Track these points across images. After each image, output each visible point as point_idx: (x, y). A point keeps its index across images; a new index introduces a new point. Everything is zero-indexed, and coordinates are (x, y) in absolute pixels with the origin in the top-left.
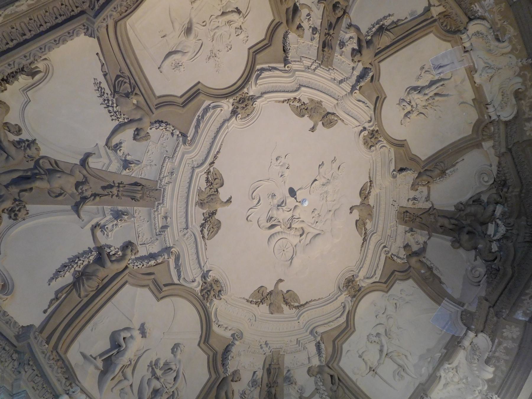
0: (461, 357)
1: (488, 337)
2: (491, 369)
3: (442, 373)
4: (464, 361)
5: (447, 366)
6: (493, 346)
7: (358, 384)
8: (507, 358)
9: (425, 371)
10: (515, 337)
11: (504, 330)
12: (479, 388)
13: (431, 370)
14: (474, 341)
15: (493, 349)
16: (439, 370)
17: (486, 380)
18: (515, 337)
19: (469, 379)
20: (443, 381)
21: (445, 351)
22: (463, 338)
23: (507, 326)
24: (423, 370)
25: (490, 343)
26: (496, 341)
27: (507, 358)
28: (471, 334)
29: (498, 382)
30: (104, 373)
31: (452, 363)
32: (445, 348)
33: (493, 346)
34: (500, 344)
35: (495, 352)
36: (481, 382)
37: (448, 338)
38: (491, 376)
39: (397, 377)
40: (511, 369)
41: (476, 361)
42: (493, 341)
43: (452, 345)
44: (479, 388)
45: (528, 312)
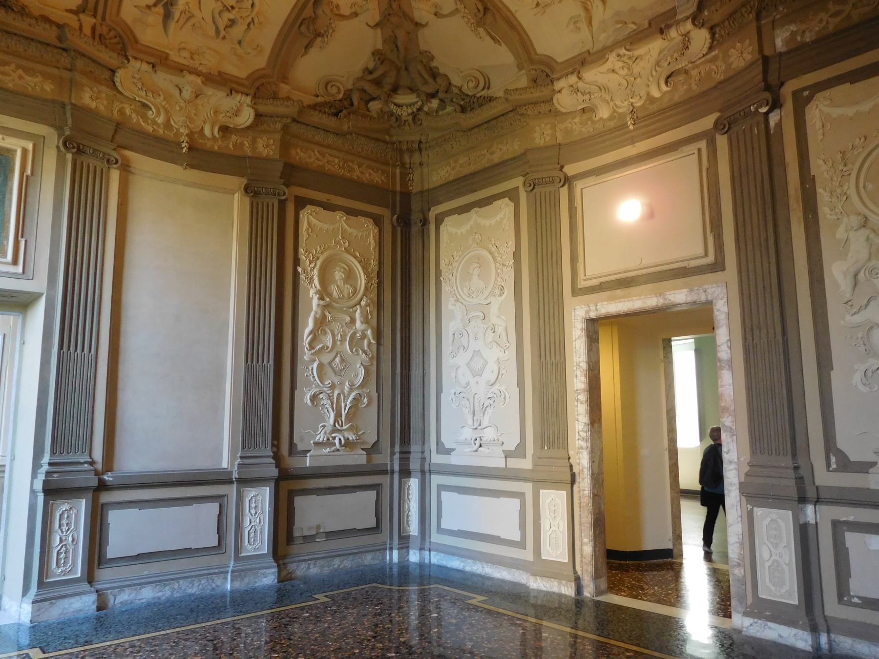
0: (654, 47)
1: (558, 107)
2: (664, 88)
3: (612, 57)
4: (655, 53)
5: (623, 51)
6: (704, 56)
7: (517, 15)
8: (694, 87)
9: (603, 39)
10: (734, 66)
11: (738, 45)
12: (631, 100)
13: (609, 42)
14: (692, 34)
15: (698, 63)
16: (611, 51)
17: (648, 94)
18: (734, 66)
19: (639, 80)
20: (608, 65)
21: (647, 25)
22: (678, 23)
23: (748, 41)
24: (603, 37)
25: (705, 50)
26: (713, 53)
27: (694, 87)
28: (689, 25)
29: (654, 108)
30: (167, 16)
31: (635, 49)
32: (650, 24)
33: (704, 56)
34: (714, 60)
35: (698, 66)
36: (643, 93)
37: (661, 10)
38: (656, 94)
39: (572, 26)
40: (677, 105)
41: (666, 64)
42: (711, 48)
43: (660, 25)
44: (631, 100)
45: (799, 38)
